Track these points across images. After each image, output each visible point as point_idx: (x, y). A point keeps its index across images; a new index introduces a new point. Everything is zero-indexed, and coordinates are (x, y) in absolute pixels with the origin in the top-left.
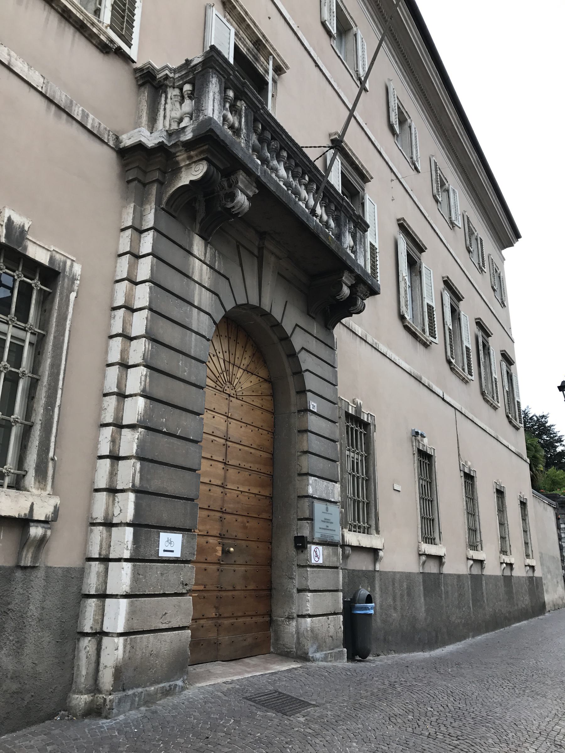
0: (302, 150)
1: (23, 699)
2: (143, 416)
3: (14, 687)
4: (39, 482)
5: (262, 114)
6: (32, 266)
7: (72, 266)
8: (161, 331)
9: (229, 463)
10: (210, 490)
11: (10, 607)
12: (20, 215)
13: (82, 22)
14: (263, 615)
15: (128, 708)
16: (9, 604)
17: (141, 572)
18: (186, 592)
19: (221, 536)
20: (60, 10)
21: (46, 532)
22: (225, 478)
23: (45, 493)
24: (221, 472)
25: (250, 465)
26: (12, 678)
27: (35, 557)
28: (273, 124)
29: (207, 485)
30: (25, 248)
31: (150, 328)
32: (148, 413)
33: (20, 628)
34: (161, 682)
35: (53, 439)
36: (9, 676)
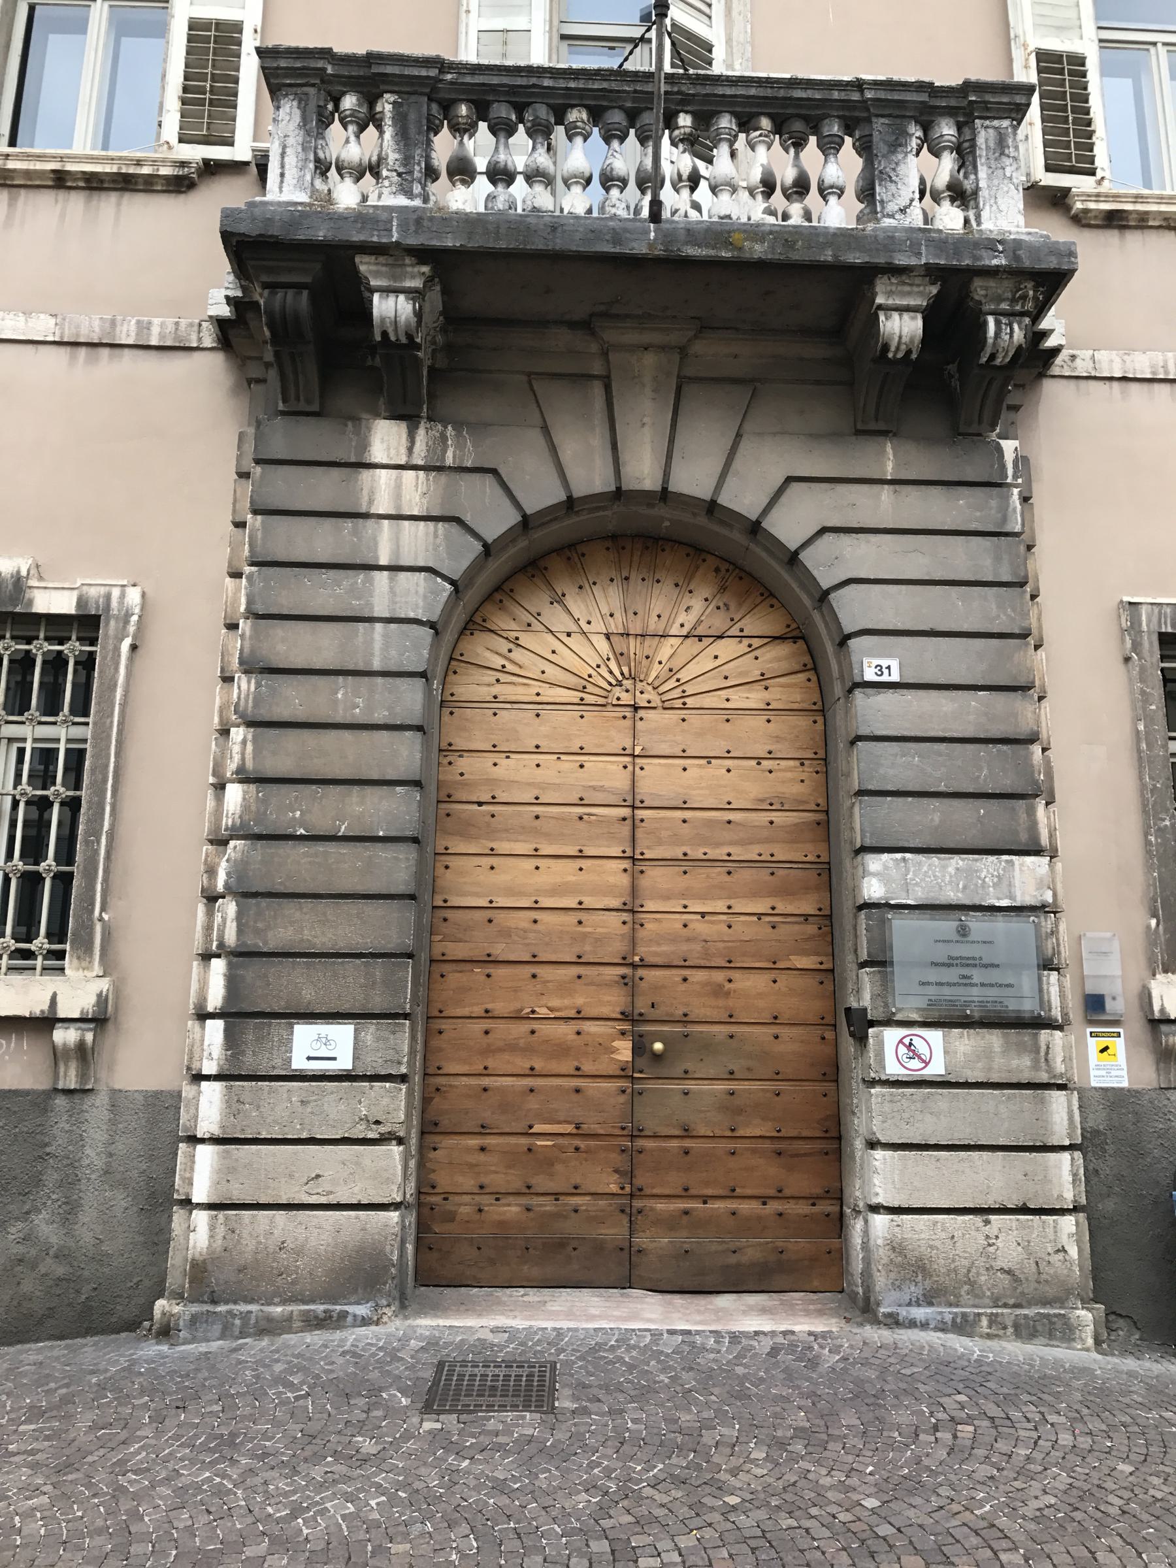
0: (626, 73)
1: (78, 1292)
2: (240, 817)
3: (61, 1270)
4: (79, 958)
5: (451, 83)
6: (57, 625)
7: (123, 596)
8: (281, 648)
9: (646, 856)
10: (580, 922)
11: (48, 1150)
12: (10, 558)
13: (119, 174)
14: (813, 1200)
15: (217, 1334)
16: (46, 1145)
17: (246, 1097)
18: (377, 1136)
19: (625, 1017)
20: (81, 184)
21: (83, 1035)
22: (634, 890)
23: (90, 974)
24: (625, 880)
25: (726, 850)
26: (56, 1257)
27: (83, 1076)
28: (495, 80)
29: (571, 913)
30: (30, 602)
31: (252, 651)
32: (253, 808)
33: (70, 1182)
34: (312, 1301)
35: (99, 887)
36: (51, 1253)
